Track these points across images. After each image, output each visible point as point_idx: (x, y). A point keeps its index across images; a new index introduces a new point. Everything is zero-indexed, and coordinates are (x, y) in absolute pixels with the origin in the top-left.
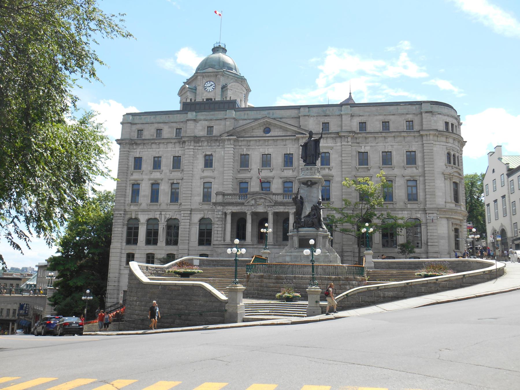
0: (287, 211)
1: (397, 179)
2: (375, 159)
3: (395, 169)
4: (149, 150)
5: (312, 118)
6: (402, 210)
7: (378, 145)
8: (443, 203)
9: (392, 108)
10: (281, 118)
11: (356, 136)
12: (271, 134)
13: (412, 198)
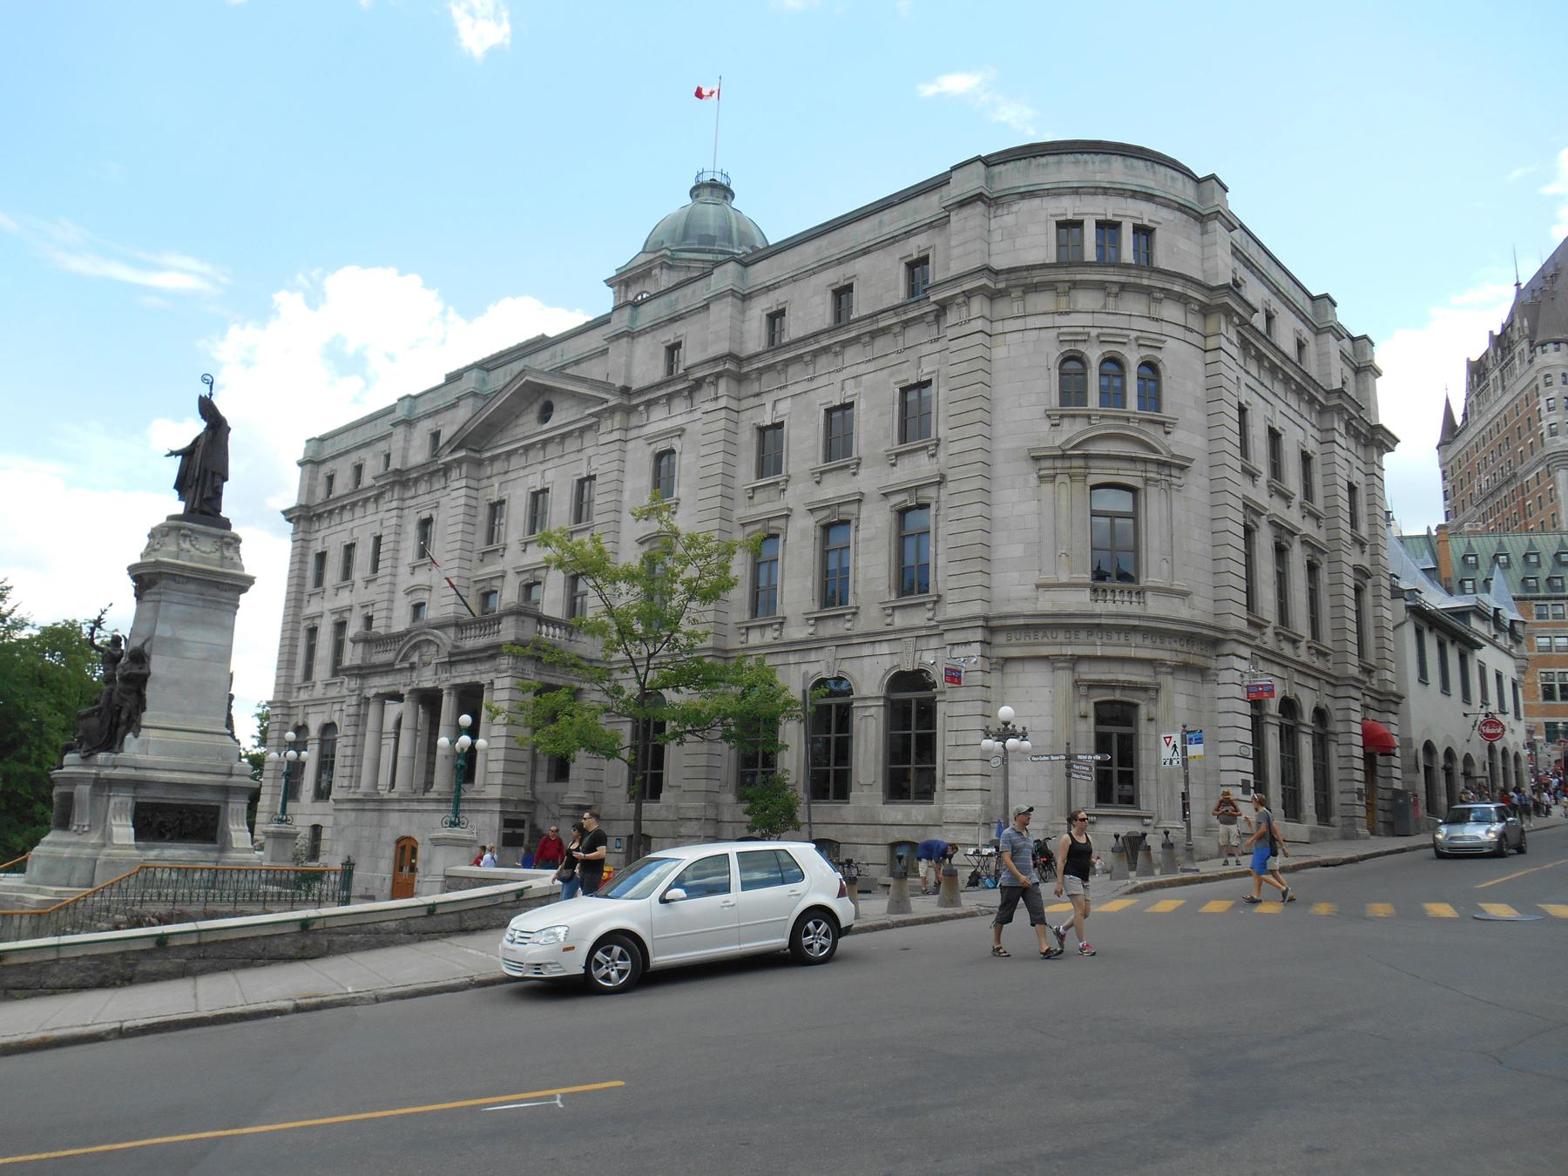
0: (477, 678)
1: (865, 511)
2: (803, 443)
3: (862, 472)
4: (339, 528)
5: (642, 339)
6: (873, 638)
7: (814, 385)
8: (1028, 590)
9: (865, 225)
10: (577, 363)
11: (745, 370)
12: (555, 420)
13: (911, 581)
